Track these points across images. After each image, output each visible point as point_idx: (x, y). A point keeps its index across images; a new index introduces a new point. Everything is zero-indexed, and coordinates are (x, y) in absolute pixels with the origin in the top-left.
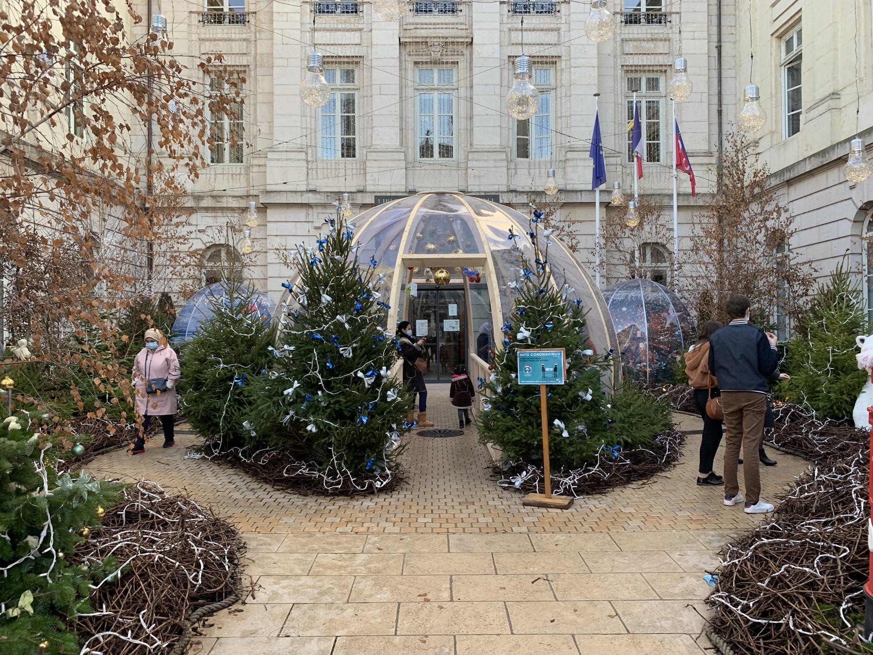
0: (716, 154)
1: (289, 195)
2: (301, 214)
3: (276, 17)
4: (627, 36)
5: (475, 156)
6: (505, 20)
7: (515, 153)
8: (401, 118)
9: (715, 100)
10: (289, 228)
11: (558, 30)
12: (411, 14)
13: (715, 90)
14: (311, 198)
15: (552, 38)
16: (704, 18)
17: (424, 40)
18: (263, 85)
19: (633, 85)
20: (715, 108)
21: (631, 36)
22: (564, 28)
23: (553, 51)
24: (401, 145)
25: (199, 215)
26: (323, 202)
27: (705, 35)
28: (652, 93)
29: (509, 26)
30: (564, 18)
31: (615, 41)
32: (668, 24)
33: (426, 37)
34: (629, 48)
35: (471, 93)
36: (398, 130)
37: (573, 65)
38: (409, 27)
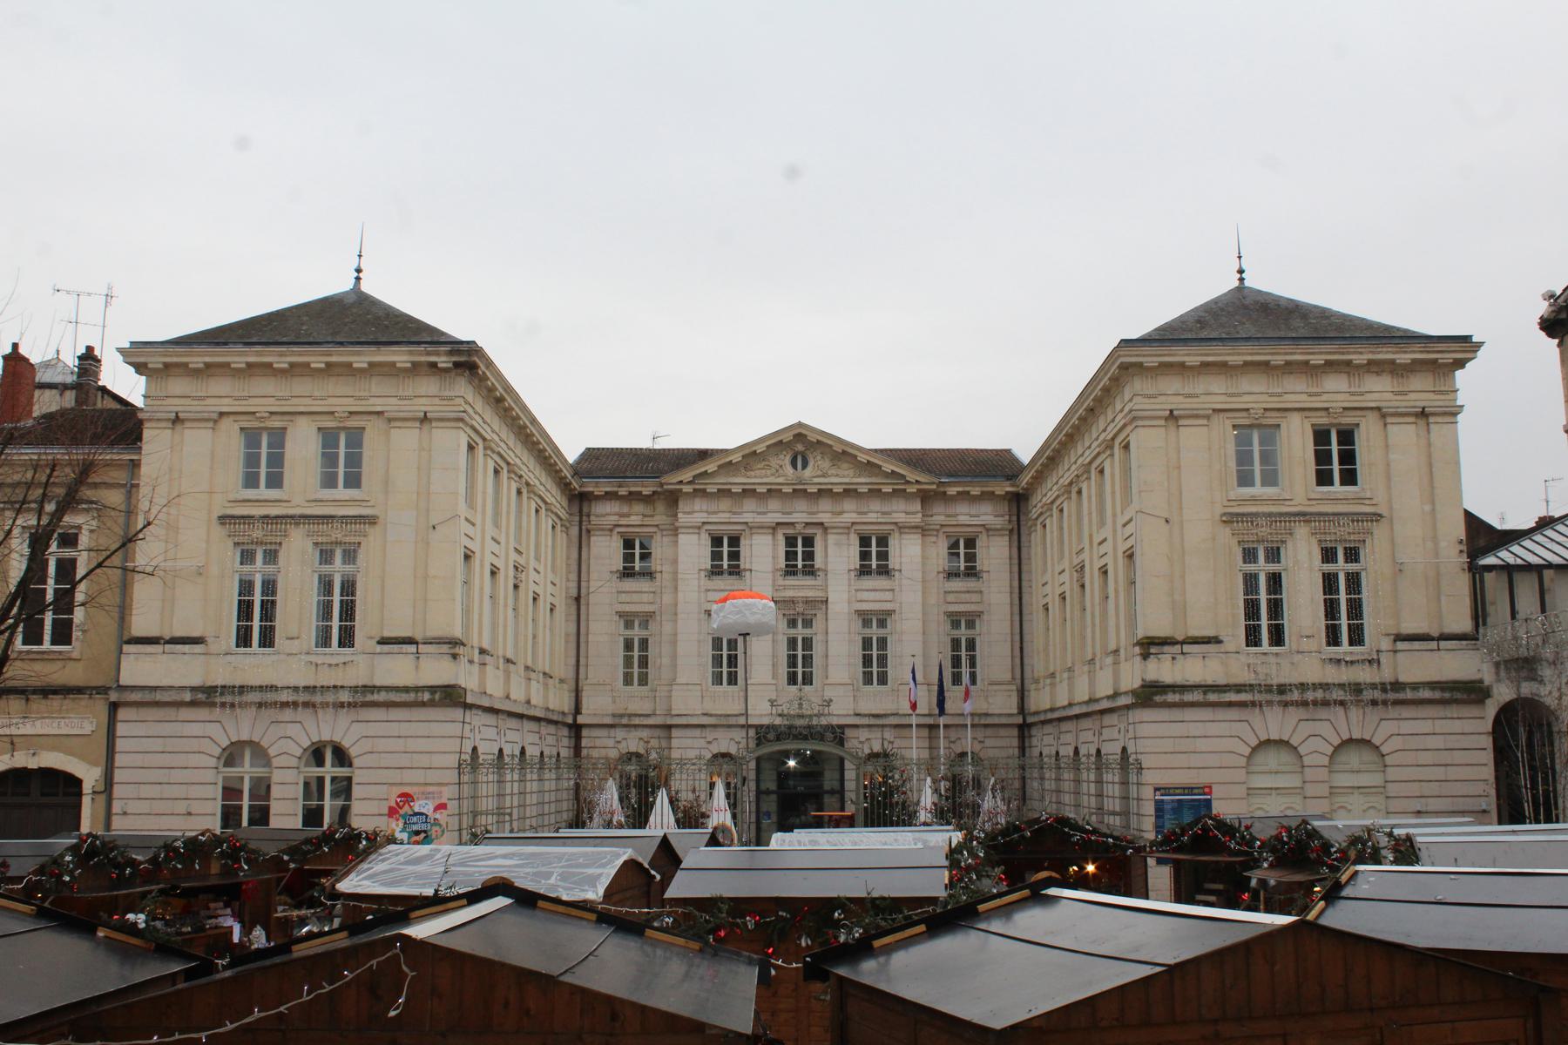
2: (697, 732)
9: (1017, 638)
10: (689, 742)
15: (888, 596)
18: (667, 628)
19: (956, 624)
20: (1017, 645)
23: (888, 606)
34: (950, 598)
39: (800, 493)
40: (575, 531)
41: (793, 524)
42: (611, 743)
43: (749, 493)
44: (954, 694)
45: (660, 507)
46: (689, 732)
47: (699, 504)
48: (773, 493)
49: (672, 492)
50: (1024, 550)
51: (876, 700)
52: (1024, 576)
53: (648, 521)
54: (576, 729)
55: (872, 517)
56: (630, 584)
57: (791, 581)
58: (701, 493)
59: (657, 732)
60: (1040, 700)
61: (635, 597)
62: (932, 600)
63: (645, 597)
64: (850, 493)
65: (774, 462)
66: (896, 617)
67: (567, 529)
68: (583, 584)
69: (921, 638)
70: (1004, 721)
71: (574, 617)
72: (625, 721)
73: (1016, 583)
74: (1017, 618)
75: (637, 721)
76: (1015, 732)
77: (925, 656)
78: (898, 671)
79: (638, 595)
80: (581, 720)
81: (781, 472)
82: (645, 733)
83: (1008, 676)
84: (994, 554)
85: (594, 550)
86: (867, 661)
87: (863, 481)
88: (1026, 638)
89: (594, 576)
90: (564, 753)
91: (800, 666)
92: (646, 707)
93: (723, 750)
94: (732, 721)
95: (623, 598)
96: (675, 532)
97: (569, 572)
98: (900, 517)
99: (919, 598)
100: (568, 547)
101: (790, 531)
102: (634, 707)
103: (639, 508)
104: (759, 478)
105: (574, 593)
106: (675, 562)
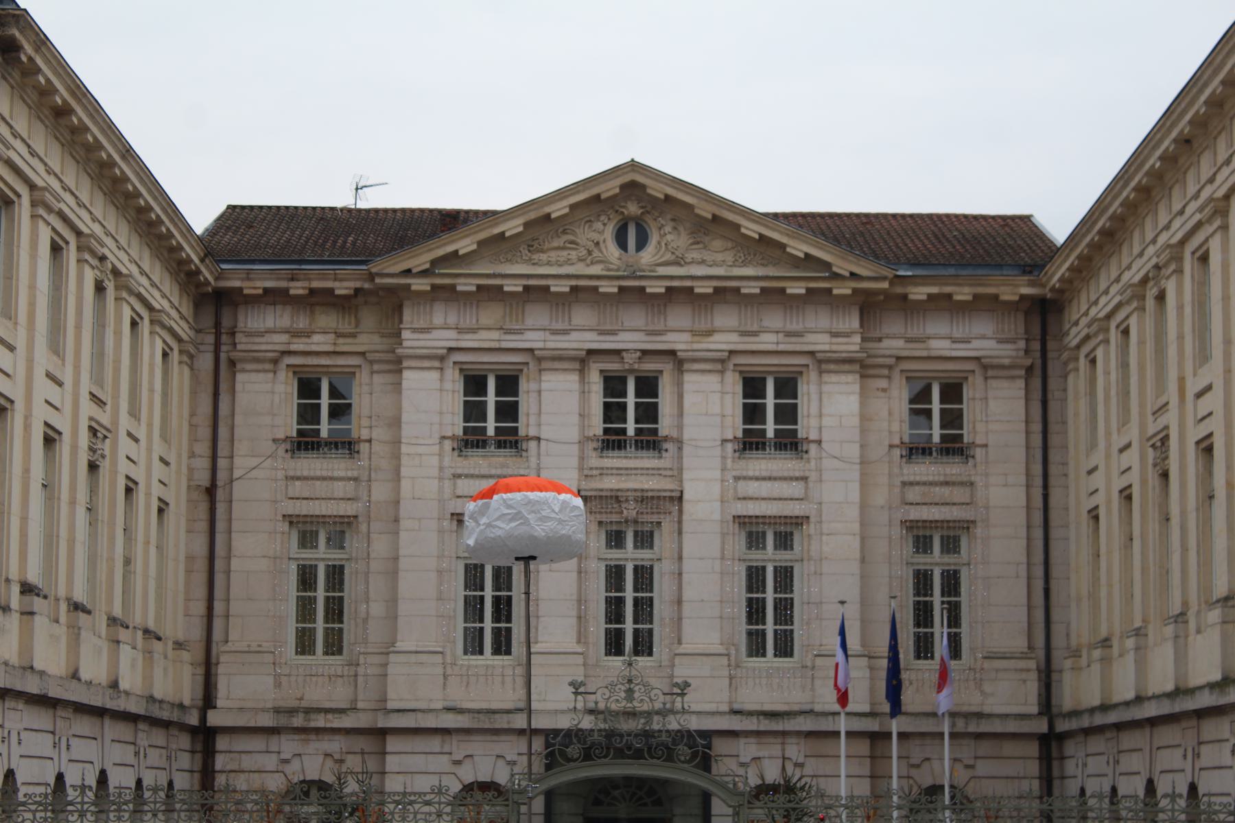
0: (1041, 653)
1: (420, 715)
2: (435, 743)
3: (404, 460)
4: (912, 478)
5: (685, 659)
6: (729, 461)
7: (743, 649)
8: (579, 601)
9: (1039, 572)
10: (417, 762)
11: (805, 479)
12: (594, 454)
13: (1039, 557)
14: (449, 721)
15: (796, 489)
16: (1021, 454)
17: (613, 494)
18: (380, 546)
19: (922, 544)
20: (1039, 585)
21: (918, 478)
22: (813, 476)
24: (579, 642)
25: (283, 738)
26: (466, 726)
27: (1023, 479)
28: (948, 559)
29: (735, 473)
30: (813, 463)
31: (891, 486)
32: (971, 460)
33: (618, 490)
35: (680, 568)
36: (574, 621)
37: (825, 531)
38: (590, 473)
39: (632, 294)
40: (205, 361)
41: (618, 352)
42: (270, 762)
43: (535, 293)
44: (919, 676)
45: (369, 319)
46: (420, 743)
47: (440, 314)
48: (582, 293)
49: (391, 290)
50: (1053, 406)
51: (770, 685)
52: (1054, 456)
53: (345, 345)
54: (205, 738)
55: (768, 341)
56: (310, 464)
57: (614, 460)
58: (445, 294)
59: (362, 743)
60: (1081, 689)
61: (320, 488)
62: (880, 497)
63: (340, 489)
64: (725, 294)
65: (585, 235)
66: (811, 529)
67: (190, 359)
68: (222, 463)
69: (855, 567)
70: (1012, 727)
71: (203, 526)
72: (298, 721)
73: (1038, 469)
74: (1038, 533)
75: (320, 721)
76: (1033, 749)
77: (865, 602)
78: (814, 630)
79: (327, 484)
80: (214, 719)
81: (598, 254)
82: (335, 745)
83: (1021, 643)
84: (997, 414)
85: (242, 399)
86: (755, 611)
87: (750, 274)
88: (1055, 572)
89: (241, 448)
90: (182, 782)
91: (629, 619)
92: (339, 695)
93: (482, 778)
94: (501, 722)
95: (298, 488)
96: (396, 365)
97: (193, 440)
98: (820, 342)
99: (855, 495)
100: (194, 393)
101: (613, 366)
102: (317, 694)
103: (327, 320)
104: (556, 265)
105: (203, 479)
106: (396, 422)
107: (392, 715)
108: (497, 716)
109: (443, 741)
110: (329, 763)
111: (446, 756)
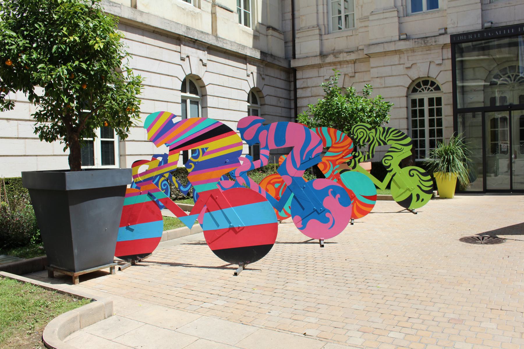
1: (386, 45)
2: (395, 59)
10: (387, 70)
46: (388, 60)
80: (294, 64)
107: (371, 47)
108: (428, 39)
109: (400, 58)
110: (347, 79)
111: (402, 66)
